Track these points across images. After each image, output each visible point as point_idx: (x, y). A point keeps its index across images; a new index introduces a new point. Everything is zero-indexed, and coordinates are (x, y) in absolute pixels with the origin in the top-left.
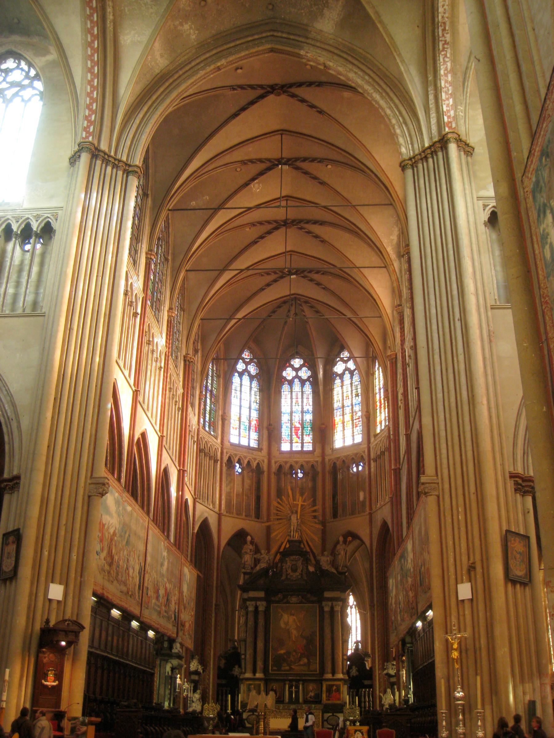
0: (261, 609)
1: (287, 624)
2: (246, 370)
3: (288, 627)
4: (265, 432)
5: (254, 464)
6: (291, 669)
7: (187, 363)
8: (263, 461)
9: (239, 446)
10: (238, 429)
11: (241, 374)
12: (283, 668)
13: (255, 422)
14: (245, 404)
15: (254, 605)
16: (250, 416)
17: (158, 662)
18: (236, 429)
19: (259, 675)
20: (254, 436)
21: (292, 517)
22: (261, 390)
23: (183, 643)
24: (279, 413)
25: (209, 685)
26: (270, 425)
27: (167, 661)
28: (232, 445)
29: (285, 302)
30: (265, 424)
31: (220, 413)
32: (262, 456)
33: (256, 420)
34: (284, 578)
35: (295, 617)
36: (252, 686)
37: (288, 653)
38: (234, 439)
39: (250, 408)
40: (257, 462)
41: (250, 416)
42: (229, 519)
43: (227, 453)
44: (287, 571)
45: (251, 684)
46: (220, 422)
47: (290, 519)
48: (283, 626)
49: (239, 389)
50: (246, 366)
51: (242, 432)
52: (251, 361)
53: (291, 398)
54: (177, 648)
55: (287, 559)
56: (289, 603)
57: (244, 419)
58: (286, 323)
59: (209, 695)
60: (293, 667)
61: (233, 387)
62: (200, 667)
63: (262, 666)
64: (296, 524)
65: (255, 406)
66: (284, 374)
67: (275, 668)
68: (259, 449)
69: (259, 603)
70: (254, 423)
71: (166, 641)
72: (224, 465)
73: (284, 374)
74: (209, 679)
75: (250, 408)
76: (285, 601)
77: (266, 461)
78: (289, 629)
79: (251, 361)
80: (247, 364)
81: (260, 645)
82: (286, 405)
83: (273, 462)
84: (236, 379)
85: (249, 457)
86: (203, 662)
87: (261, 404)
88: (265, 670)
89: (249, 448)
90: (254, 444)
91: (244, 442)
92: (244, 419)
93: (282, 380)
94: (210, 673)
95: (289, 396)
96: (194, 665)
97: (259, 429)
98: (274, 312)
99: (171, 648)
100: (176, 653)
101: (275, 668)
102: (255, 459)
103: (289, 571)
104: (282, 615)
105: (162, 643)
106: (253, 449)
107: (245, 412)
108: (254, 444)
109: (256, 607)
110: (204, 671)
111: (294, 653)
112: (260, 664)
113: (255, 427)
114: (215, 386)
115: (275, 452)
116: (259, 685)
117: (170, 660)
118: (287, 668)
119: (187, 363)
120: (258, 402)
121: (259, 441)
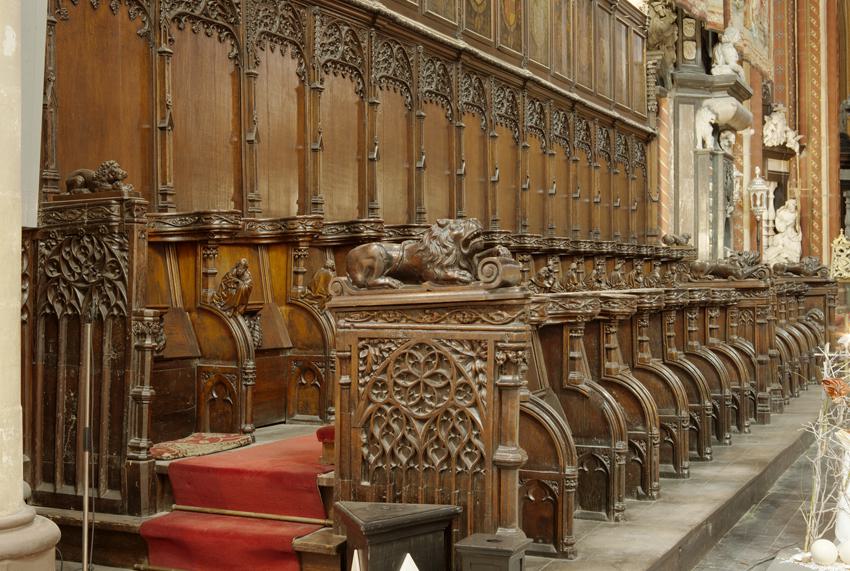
17: (667, 109)
23: (746, 51)
25: (819, 185)
27: (697, 104)
54: (726, 61)
59: (820, 209)
62: (791, 134)
71: (693, 40)
74: (818, 171)
86: (798, 123)
94: (819, 150)
96: (777, 131)
99: (708, 63)
100: (728, 78)
105: (678, 47)
110: (802, 148)
117: (706, 102)
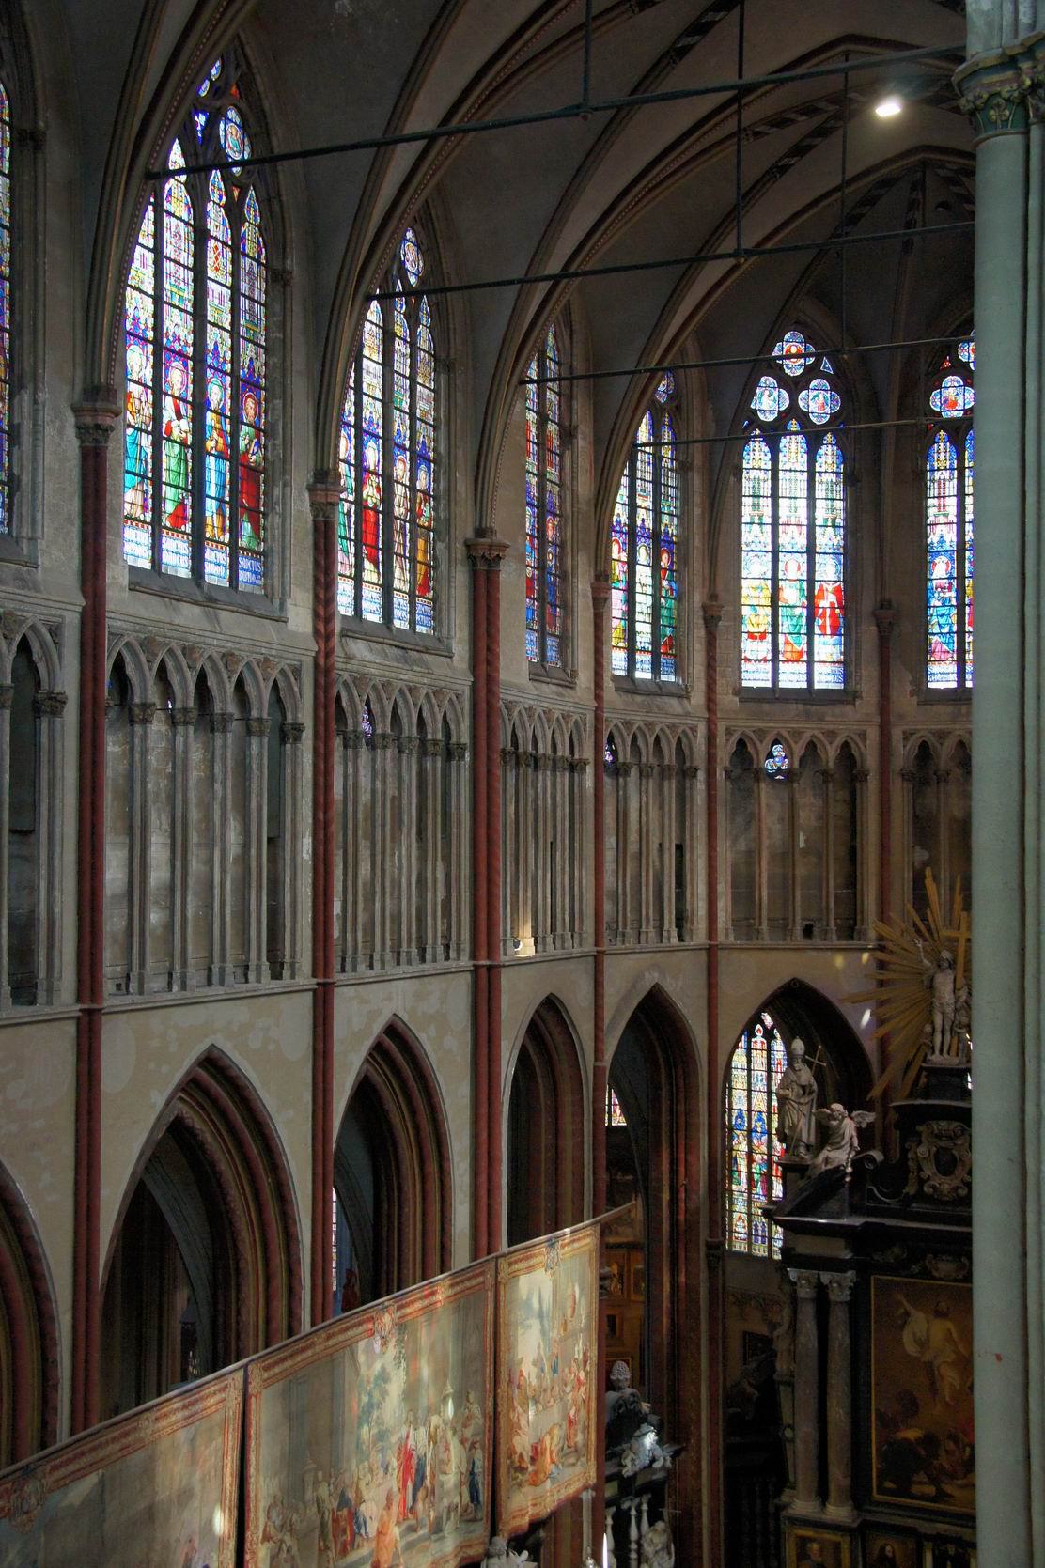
0: (840, 1295)
1: (923, 1344)
2: (793, 411)
3: (927, 1357)
4: (869, 632)
5: (831, 753)
6: (941, 1496)
7: (481, 567)
8: (863, 736)
9: (775, 695)
10: (769, 637)
11: (772, 435)
12: (915, 1489)
13: (832, 598)
14: (793, 538)
15: (814, 1281)
16: (811, 580)
18: (763, 636)
19: (838, 1512)
20: (828, 648)
21: (939, 978)
22: (851, 478)
24: (921, 554)
26: (884, 604)
28: (758, 696)
29: (887, 183)
30: (868, 604)
31: (698, 598)
32: (859, 721)
33: (837, 591)
34: (911, 1189)
35: (950, 1325)
36: (815, 1546)
37: (930, 1441)
38: (756, 676)
39: (811, 551)
40: (839, 741)
41: (811, 580)
42: (744, 955)
43: (729, 732)
44: (920, 1169)
45: (811, 1540)
46: (700, 632)
47: (931, 987)
48: (911, 1348)
49: (766, 489)
50: (795, 384)
51: (788, 641)
52: (811, 372)
53: (961, 495)
55: (920, 1128)
56: (926, 1274)
57: (791, 594)
58: (907, 246)
60: (948, 1489)
61: (747, 487)
63: (847, 1482)
64: (949, 1010)
65: (829, 539)
66: (935, 402)
67: (889, 1485)
68: (844, 697)
69: (826, 1277)
70: (828, 601)
72: (720, 775)
73: (935, 402)
75: (811, 551)
76: (915, 1269)
77: (873, 734)
78: (930, 1364)
79: (811, 372)
80: (794, 386)
81: (838, 1413)
82: (942, 519)
83: (897, 734)
84: (756, 455)
85: (811, 730)
87: (852, 528)
88: (858, 1495)
89: (809, 696)
90: (826, 678)
91: (792, 677)
92: (791, 594)
93: (925, 428)
95: (951, 488)
97: (847, 625)
98: (853, 220)
101: (889, 1485)
102: (831, 735)
103: (929, 1171)
104: (907, 1314)
106: (827, 697)
107: (793, 567)
108: (826, 678)
109: (821, 1290)
111: (951, 1446)
112: (838, 1476)
113: (833, 616)
114: (669, 506)
115: (903, 700)
116: (837, 1546)
118: (930, 1490)
119: (481, 567)
120: (839, 522)
121: (849, 665)
